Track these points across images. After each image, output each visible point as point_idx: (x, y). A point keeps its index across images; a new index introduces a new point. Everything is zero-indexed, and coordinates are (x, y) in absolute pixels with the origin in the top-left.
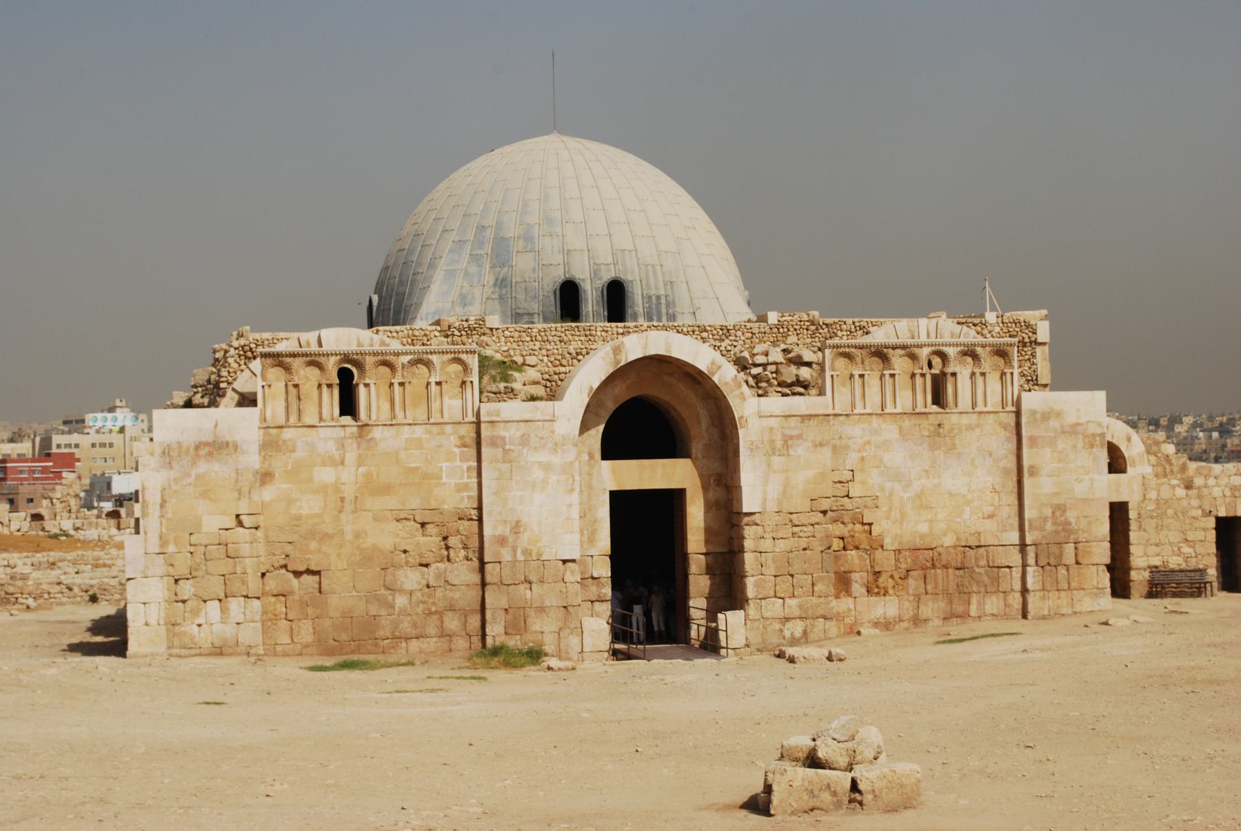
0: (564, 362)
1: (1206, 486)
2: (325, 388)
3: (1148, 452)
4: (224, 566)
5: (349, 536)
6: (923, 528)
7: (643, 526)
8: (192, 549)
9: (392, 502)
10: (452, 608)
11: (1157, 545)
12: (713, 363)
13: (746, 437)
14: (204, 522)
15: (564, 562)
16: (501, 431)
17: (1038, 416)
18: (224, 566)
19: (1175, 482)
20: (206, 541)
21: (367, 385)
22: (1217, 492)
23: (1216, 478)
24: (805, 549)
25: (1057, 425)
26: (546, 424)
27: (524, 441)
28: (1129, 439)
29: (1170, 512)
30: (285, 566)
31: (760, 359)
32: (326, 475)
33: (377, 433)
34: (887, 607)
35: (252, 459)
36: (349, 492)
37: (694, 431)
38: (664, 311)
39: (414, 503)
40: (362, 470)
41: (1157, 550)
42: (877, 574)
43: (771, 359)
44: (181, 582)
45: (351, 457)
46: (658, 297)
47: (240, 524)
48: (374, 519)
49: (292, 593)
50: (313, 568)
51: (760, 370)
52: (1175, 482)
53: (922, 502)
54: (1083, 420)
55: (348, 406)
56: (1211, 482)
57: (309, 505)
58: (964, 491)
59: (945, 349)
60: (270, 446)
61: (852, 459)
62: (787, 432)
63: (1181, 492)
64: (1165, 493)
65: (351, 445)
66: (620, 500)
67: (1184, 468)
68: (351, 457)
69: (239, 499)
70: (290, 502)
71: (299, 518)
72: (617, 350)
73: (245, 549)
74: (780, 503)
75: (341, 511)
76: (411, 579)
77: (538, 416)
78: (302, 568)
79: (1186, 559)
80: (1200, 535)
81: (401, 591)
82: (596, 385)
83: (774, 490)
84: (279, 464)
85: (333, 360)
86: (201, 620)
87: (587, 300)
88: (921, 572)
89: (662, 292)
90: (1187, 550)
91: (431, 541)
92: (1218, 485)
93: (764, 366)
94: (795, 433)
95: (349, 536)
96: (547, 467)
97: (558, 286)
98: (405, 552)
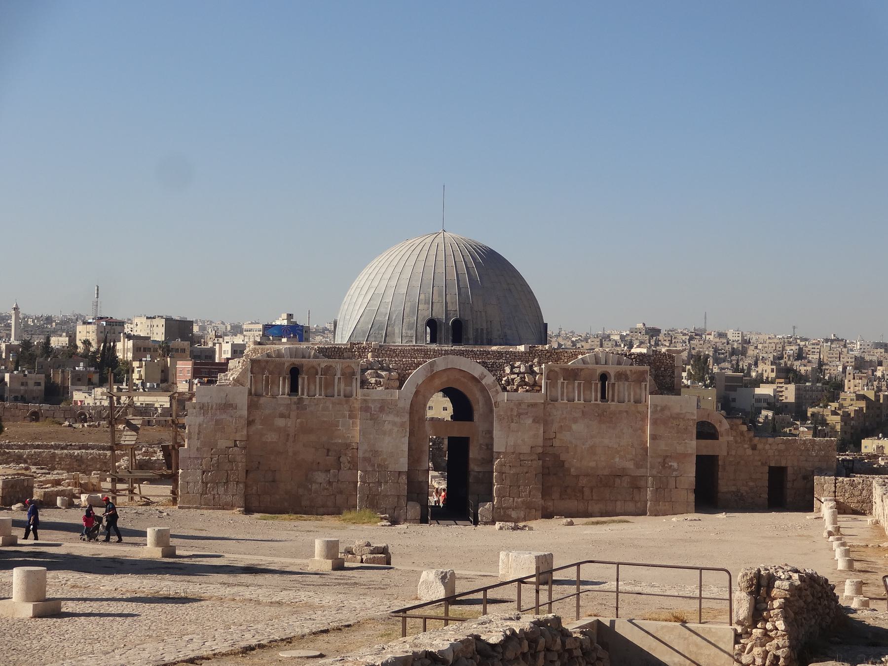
1: (764, 449)
3: (731, 428)
5: (290, 454)
6: (592, 464)
10: (341, 492)
12: (482, 374)
17: (659, 408)
19: (746, 446)
22: (770, 453)
25: (669, 414)
27: (382, 409)
29: (742, 462)
31: (516, 370)
32: (280, 422)
34: (572, 504)
35: (245, 413)
37: (475, 407)
38: (485, 336)
40: (298, 420)
45: (293, 414)
46: (482, 329)
47: (236, 446)
51: (516, 376)
52: (746, 446)
53: (592, 450)
54: (684, 412)
55: (294, 389)
56: (767, 447)
57: (271, 437)
58: (616, 446)
60: (253, 406)
61: (555, 426)
62: (521, 411)
63: (749, 452)
67: (751, 440)
68: (293, 414)
73: (238, 458)
75: (287, 440)
76: (320, 477)
83: (511, 442)
87: (441, 330)
89: (485, 326)
90: (751, 484)
92: (771, 449)
93: (518, 374)
95: (290, 454)
96: (394, 424)
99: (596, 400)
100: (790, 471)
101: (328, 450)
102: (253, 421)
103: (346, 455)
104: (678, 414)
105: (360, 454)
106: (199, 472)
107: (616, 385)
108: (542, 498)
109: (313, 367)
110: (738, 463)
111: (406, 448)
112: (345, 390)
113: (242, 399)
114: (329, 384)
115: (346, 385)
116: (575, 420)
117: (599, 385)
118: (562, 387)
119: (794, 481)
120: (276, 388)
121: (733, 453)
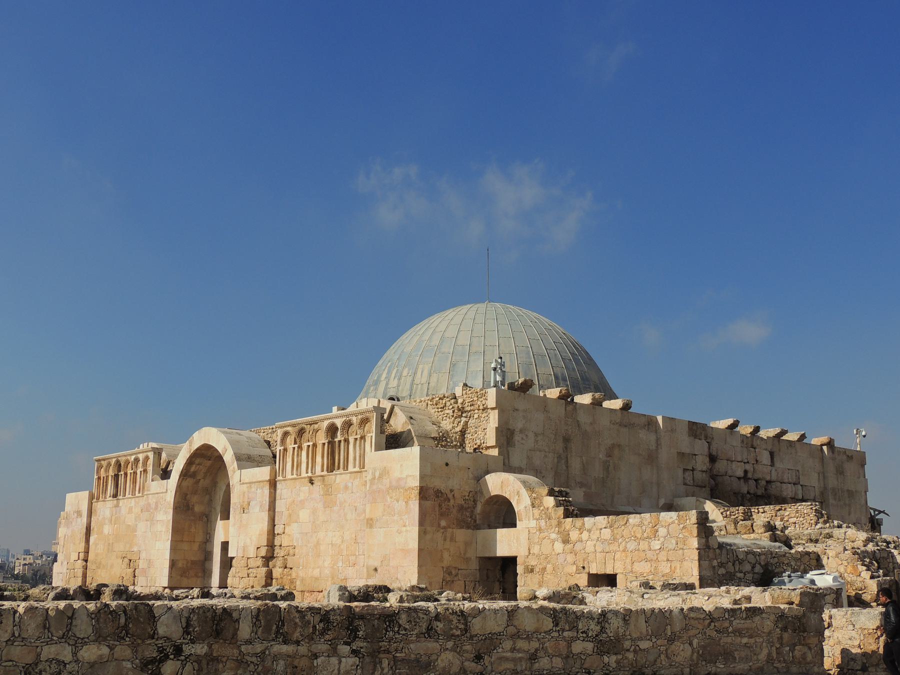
3: (533, 506)
17: (377, 474)
23: (589, 531)
28: (518, 493)
29: (549, 567)
52: (553, 536)
56: (585, 535)
63: (559, 546)
64: (546, 549)
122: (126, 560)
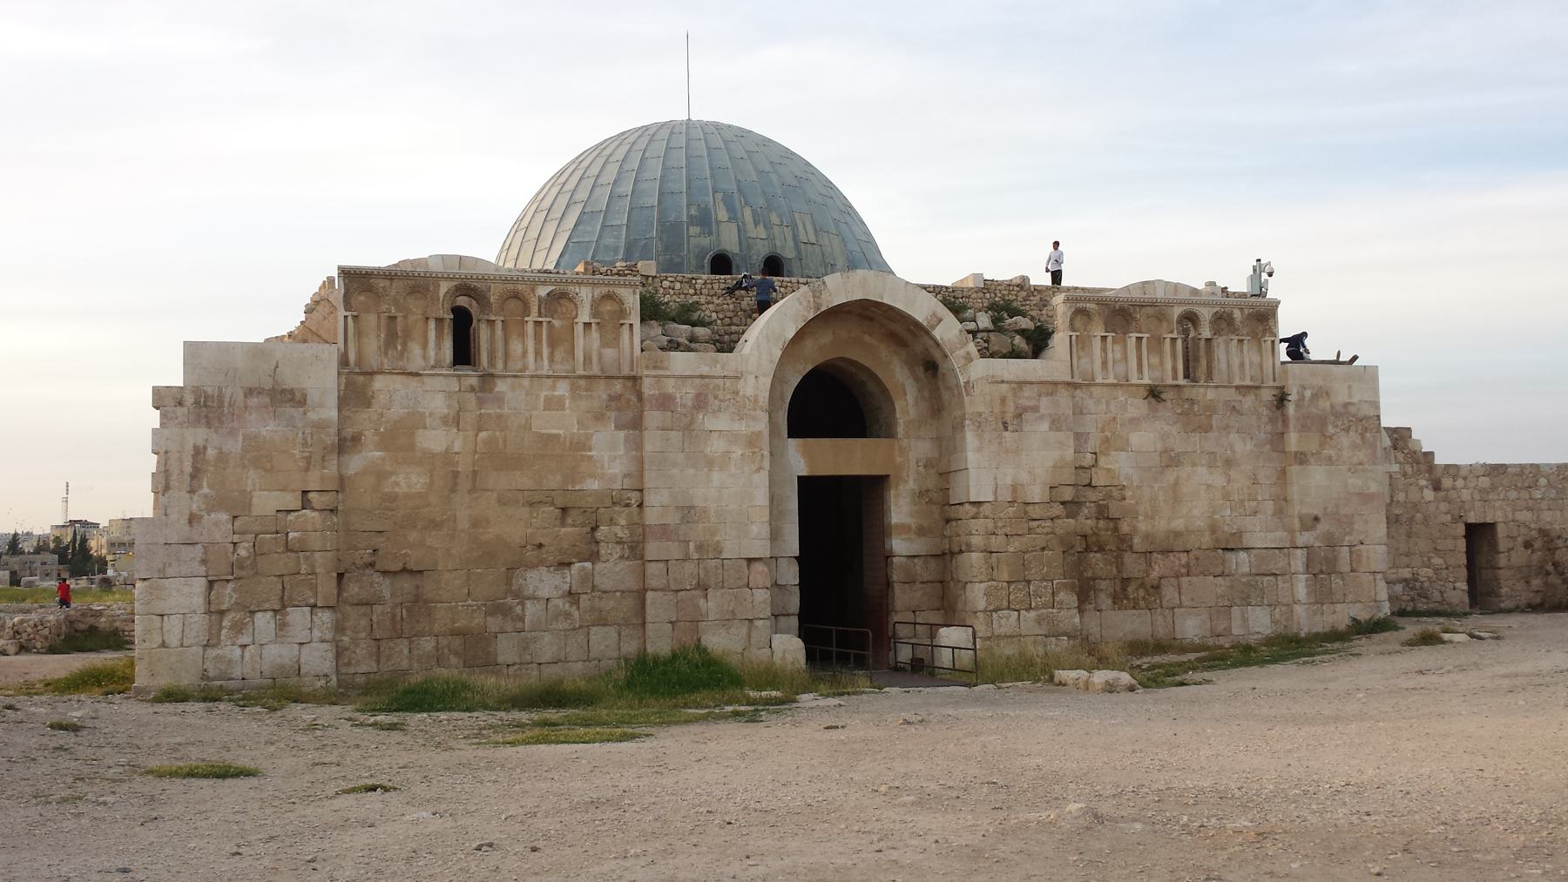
0: (735, 320)
2: (432, 324)
4: (283, 563)
5: (464, 524)
6: (1178, 524)
7: (836, 522)
8: (236, 538)
9: (523, 480)
10: (603, 622)
11: (1407, 555)
12: (934, 314)
13: (975, 404)
14: (255, 501)
15: (750, 561)
16: (670, 386)
17: (1308, 393)
18: (283, 563)
20: (257, 528)
21: (491, 323)
22: (1466, 495)
23: (1465, 479)
24: (1043, 549)
26: (728, 383)
27: (701, 403)
30: (372, 565)
32: (434, 440)
33: (501, 386)
35: (333, 414)
36: (464, 466)
39: (554, 481)
40: (483, 435)
41: (1405, 560)
42: (1126, 581)
43: (981, 326)
44: (216, 586)
48: (501, 501)
49: (380, 601)
50: (412, 566)
54: (1355, 400)
55: (464, 354)
56: (1460, 483)
57: (409, 481)
59: (1196, 309)
60: (354, 393)
63: (1429, 494)
64: (1414, 496)
65: (471, 398)
66: (807, 485)
68: (469, 418)
69: (307, 470)
70: (381, 475)
71: (393, 498)
72: (816, 294)
73: (315, 541)
74: (1015, 488)
75: (453, 490)
76: (544, 583)
77: (718, 371)
78: (397, 567)
79: (1437, 570)
80: (1449, 544)
81: (534, 598)
82: (791, 334)
83: (1007, 477)
84: (364, 421)
85: (444, 287)
86: (245, 639)
88: (1173, 580)
90: (1437, 561)
91: (571, 531)
92: (1466, 487)
94: (1031, 403)
95: (464, 524)
97: (707, 261)
98: (540, 546)
99: (1175, 377)
100: (1501, 531)
101: (564, 510)
102: (356, 439)
103: (612, 522)
104: (1346, 405)
105: (652, 517)
106: (200, 584)
107: (1215, 343)
108: (1081, 611)
109: (516, 296)
110: (1412, 519)
111: (761, 498)
112: (600, 356)
113: (321, 379)
114: (560, 340)
115: (604, 344)
116: (1134, 422)
117: (1179, 343)
118: (1104, 350)
119: (1510, 550)
120: (415, 349)
121: (1401, 497)
122: (550, 511)
